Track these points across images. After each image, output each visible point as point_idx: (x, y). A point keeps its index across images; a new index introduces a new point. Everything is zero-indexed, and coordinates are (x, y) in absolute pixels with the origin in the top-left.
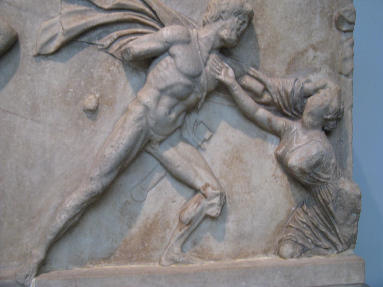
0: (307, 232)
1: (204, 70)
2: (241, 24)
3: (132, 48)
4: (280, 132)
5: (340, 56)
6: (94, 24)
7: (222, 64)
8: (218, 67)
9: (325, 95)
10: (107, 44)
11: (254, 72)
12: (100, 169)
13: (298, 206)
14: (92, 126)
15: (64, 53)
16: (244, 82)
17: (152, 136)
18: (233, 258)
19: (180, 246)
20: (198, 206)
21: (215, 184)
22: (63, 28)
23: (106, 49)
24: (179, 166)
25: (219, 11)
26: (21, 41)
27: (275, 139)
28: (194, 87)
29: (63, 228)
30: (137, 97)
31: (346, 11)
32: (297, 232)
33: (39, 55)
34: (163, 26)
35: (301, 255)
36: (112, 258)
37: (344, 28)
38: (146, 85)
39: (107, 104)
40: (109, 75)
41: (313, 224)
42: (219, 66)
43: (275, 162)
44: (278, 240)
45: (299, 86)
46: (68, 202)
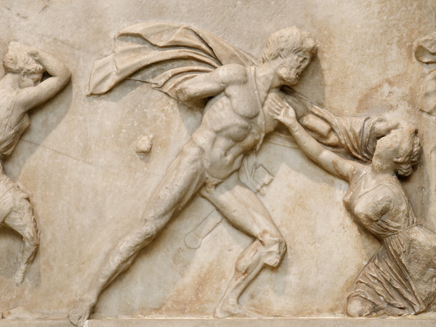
0: (379, 288)
1: (261, 110)
2: (302, 62)
3: (187, 88)
4: (348, 177)
5: (421, 91)
6: (149, 63)
7: (282, 103)
8: (277, 107)
9: (396, 136)
10: (161, 82)
11: (319, 111)
12: (155, 211)
13: (370, 261)
14: (145, 169)
15: (116, 92)
16: (307, 122)
17: (207, 178)
18: (295, 315)
19: (236, 297)
20: (255, 254)
21: (273, 231)
22: (116, 67)
23: (160, 88)
24: (235, 211)
25: (278, 49)
26: (74, 80)
27: (343, 184)
28: (251, 129)
29: (116, 272)
30: (192, 139)
31: (426, 41)
32: (367, 288)
33: (92, 94)
34: (220, 63)
35: (371, 314)
36: (164, 309)
37: (426, 60)
38: (202, 126)
39: (161, 145)
40: (163, 115)
41: (386, 280)
42: (278, 105)
43: (344, 210)
44: (346, 297)
45: (369, 126)
46: (121, 245)
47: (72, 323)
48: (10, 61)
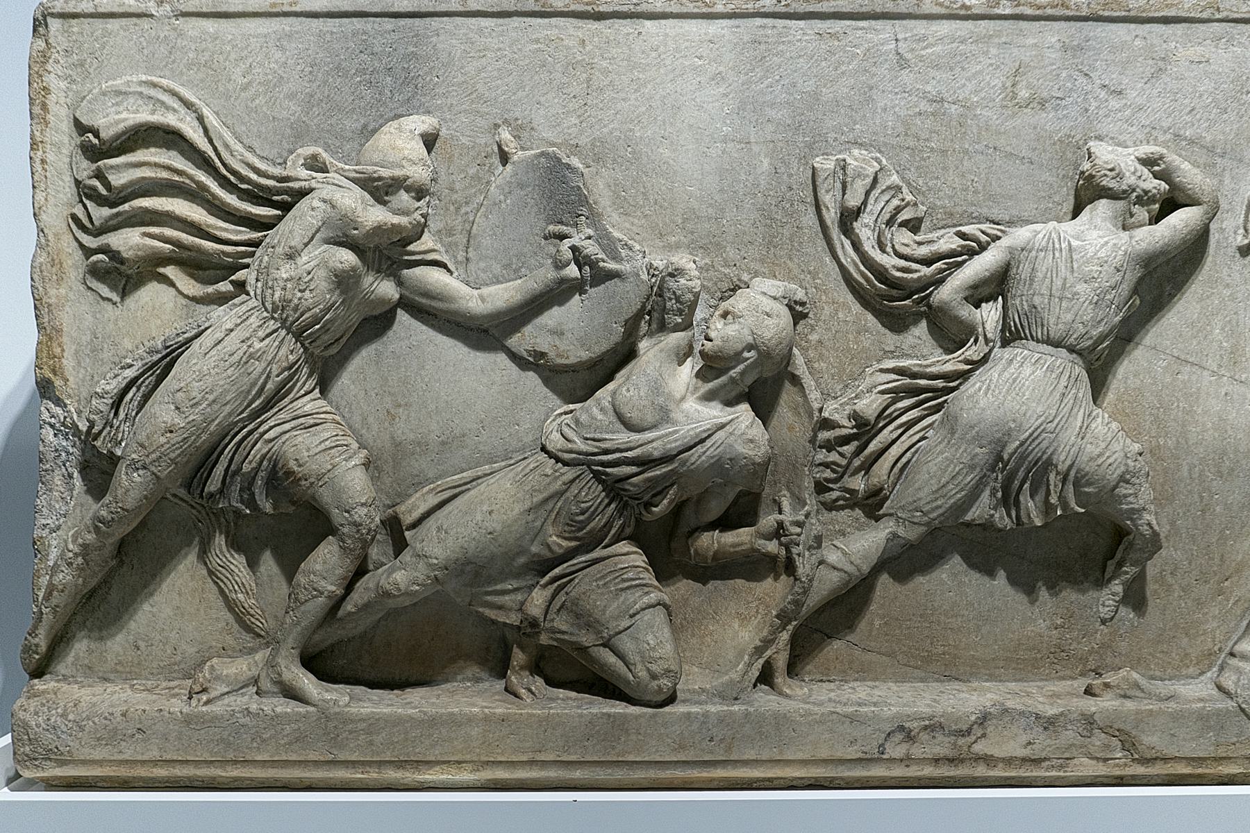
47: (1243, 710)
48: (1108, 173)
